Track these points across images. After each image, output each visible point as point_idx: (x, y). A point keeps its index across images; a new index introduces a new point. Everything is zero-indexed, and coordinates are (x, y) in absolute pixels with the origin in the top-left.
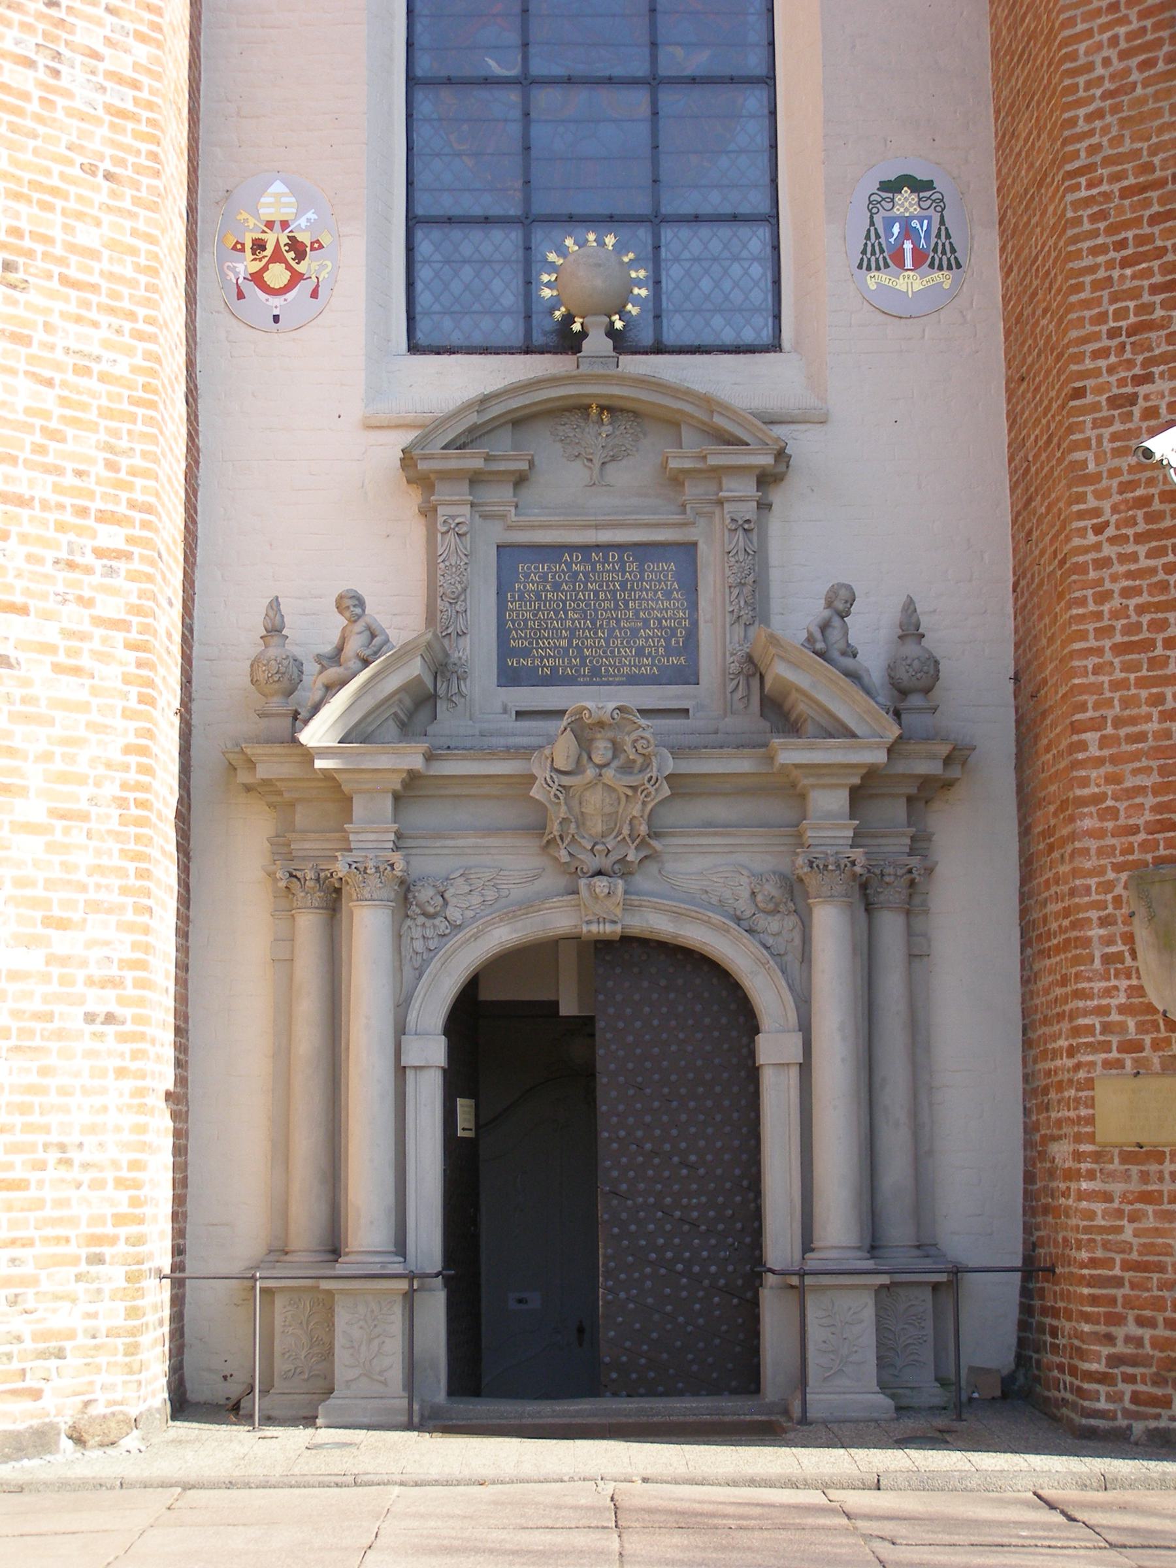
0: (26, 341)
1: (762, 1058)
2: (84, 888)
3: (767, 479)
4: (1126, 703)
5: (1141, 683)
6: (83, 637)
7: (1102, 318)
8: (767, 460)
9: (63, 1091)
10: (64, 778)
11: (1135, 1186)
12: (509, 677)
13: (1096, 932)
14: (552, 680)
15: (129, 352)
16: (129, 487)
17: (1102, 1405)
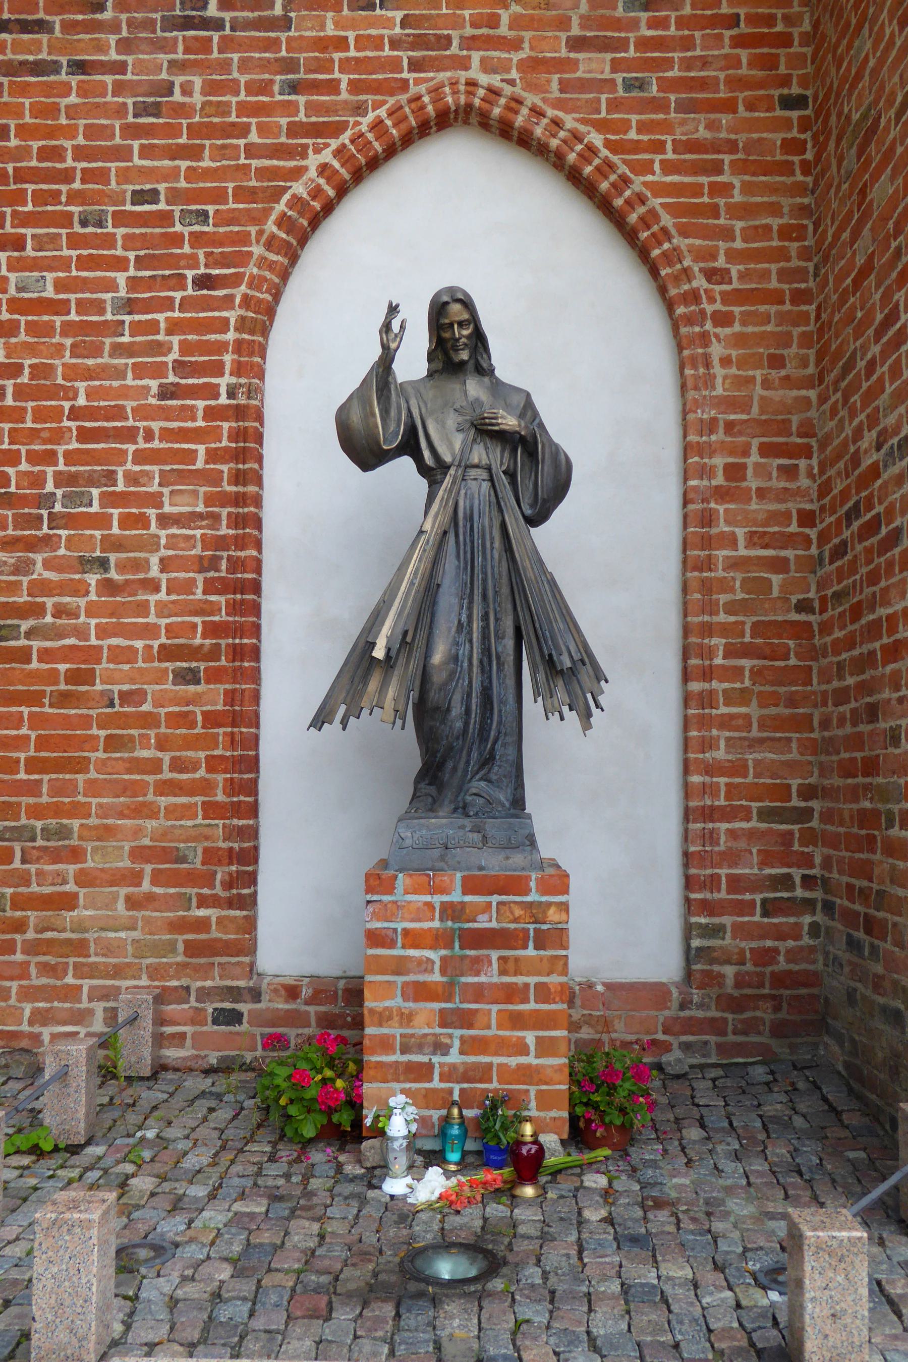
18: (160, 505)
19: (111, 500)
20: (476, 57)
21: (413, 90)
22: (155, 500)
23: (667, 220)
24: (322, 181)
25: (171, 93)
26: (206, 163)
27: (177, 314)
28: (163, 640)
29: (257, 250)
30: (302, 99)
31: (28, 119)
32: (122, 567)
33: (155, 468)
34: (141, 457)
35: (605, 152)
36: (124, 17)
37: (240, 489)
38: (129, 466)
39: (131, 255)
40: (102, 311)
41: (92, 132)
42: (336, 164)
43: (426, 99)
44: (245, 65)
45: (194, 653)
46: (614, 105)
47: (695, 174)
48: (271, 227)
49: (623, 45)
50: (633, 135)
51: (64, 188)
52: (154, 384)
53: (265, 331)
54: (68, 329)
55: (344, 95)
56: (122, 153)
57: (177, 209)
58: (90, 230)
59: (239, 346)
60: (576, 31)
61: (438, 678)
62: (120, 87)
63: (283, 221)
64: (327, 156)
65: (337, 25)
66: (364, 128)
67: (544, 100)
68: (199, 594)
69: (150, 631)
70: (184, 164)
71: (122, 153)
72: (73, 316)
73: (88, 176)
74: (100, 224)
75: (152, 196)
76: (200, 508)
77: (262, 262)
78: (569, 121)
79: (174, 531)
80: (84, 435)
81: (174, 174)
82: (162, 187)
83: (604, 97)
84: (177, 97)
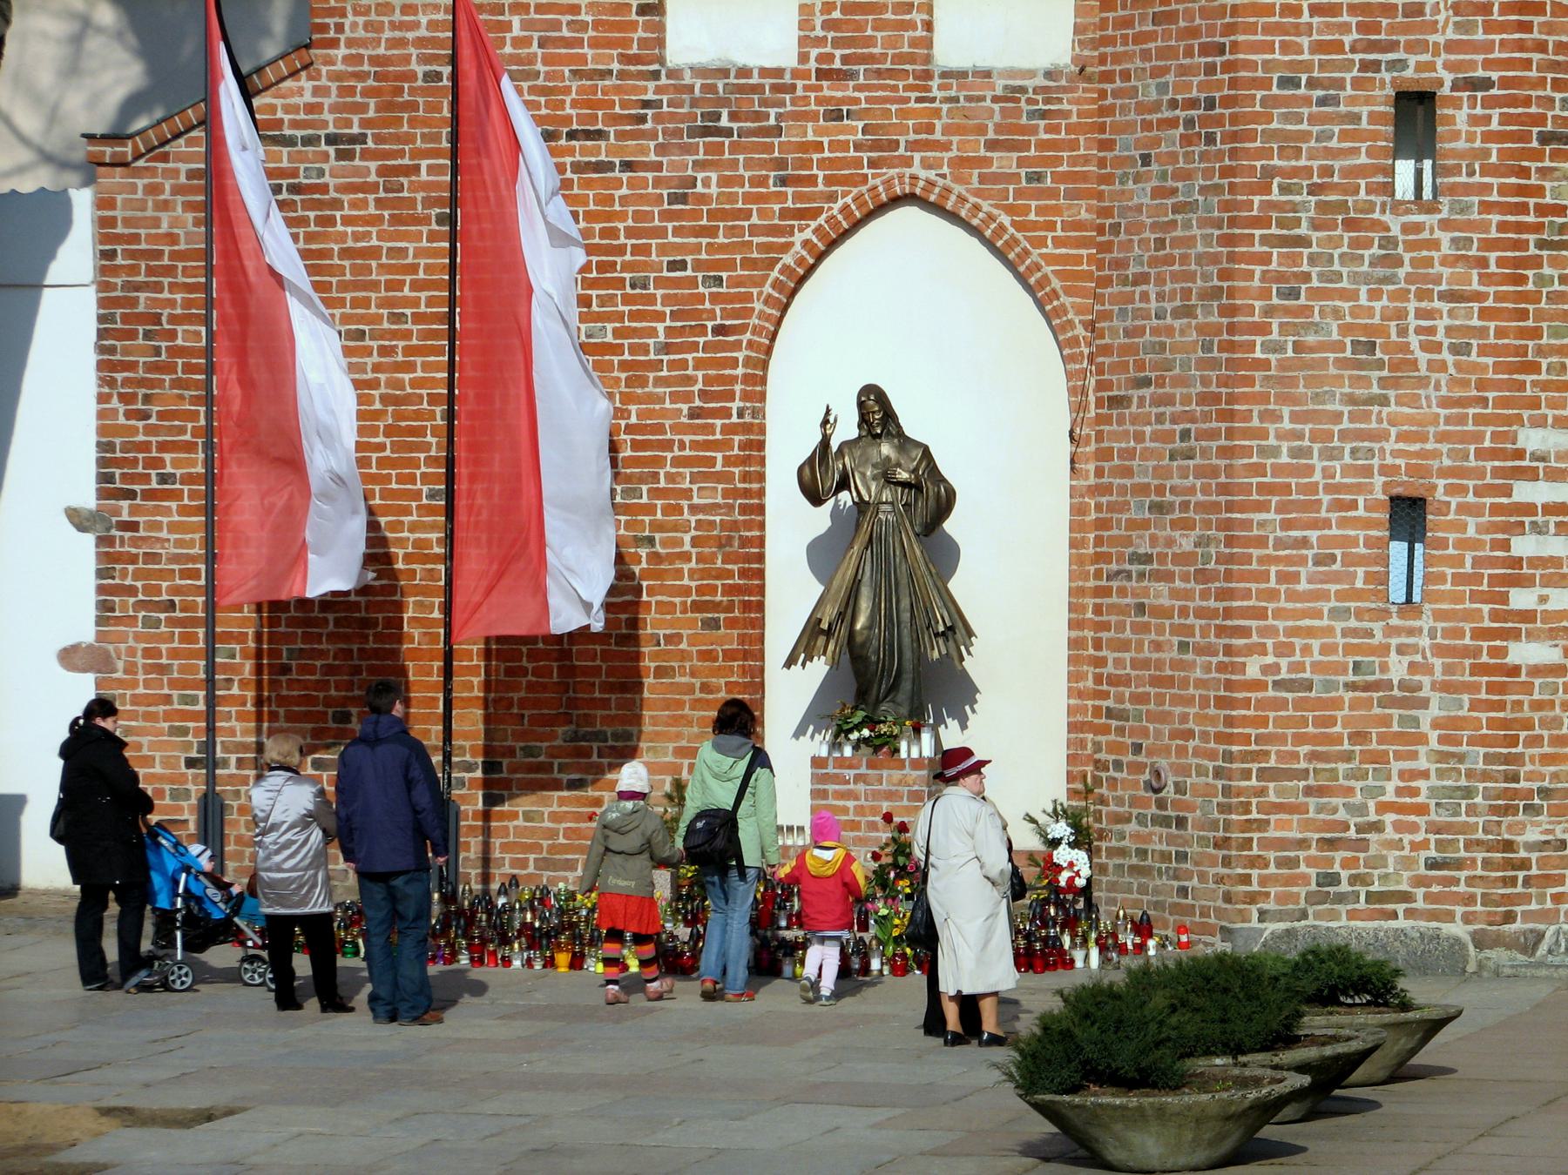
18: (691, 498)
19: (656, 493)
20: (917, 156)
21: (871, 182)
22: (687, 494)
23: (1056, 283)
24: (804, 253)
25: (695, 186)
26: (721, 240)
27: (701, 354)
28: (694, 597)
29: (758, 306)
30: (790, 190)
31: (592, 207)
32: (664, 543)
33: (687, 471)
34: (677, 462)
35: (1011, 230)
36: (660, 127)
37: (747, 486)
38: (668, 468)
39: (668, 310)
40: (647, 353)
41: (638, 216)
42: (815, 240)
43: (881, 189)
44: (748, 165)
45: (716, 607)
46: (1019, 194)
47: (1078, 247)
48: (767, 289)
49: (1025, 146)
50: (1032, 217)
51: (619, 260)
52: (685, 407)
53: (765, 365)
54: (624, 366)
55: (821, 187)
56: (661, 233)
57: (700, 275)
58: (638, 291)
59: (747, 379)
60: (991, 135)
61: (859, 639)
62: (658, 182)
63: (776, 285)
64: (808, 234)
65: (815, 133)
66: (835, 212)
67: (968, 191)
68: (719, 564)
69: (686, 591)
70: (705, 241)
71: (661, 233)
72: (627, 356)
73: (637, 250)
74: (645, 287)
75: (682, 265)
76: (719, 500)
77: (762, 315)
78: (986, 206)
79: (701, 517)
81: (697, 249)
82: (689, 259)
83: (1011, 188)
84: (700, 189)
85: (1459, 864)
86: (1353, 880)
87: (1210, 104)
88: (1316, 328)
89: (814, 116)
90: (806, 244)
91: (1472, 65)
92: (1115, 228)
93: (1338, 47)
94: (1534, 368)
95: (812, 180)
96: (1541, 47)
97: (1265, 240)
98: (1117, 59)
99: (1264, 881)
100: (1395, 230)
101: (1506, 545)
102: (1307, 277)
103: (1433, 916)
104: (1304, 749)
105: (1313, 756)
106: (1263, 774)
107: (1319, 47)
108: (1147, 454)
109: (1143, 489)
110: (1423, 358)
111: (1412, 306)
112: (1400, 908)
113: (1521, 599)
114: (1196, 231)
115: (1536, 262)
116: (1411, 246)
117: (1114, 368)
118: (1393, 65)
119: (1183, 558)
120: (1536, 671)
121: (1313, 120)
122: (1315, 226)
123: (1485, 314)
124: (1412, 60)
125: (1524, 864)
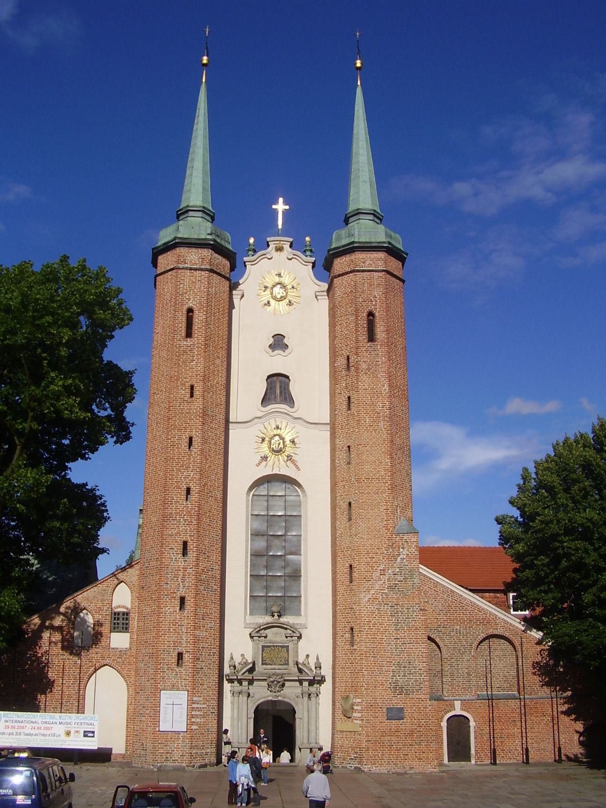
0: (204, 627)
1: (296, 717)
2: (210, 696)
3: (300, 637)
4: (342, 675)
5: (344, 673)
6: (211, 664)
7: (340, 625)
8: (299, 635)
9: (208, 722)
10: (208, 682)
11: (341, 736)
12: (263, 664)
13: (337, 704)
14: (269, 664)
15: (216, 626)
16: (216, 644)
17: (336, 763)
19: (70, 704)
22: (74, 704)
29: (85, 678)
62: (72, 661)
71: (72, 668)
73: (69, 670)
75: (75, 673)
78: (117, 666)
80: (68, 697)
85: (185, 756)
86: (170, 758)
87: (153, 653)
88: (166, 683)
89: (94, 653)
90: (92, 670)
91: (188, 649)
92: (138, 670)
93: (170, 646)
94: (195, 689)
95: (93, 662)
96: (196, 647)
97: (160, 672)
98: (139, 647)
99: (158, 758)
100: (177, 671)
101: (191, 713)
102: (165, 677)
103: (180, 763)
104: (164, 740)
105: (165, 741)
106: (158, 743)
107: (168, 646)
108: (142, 700)
109: (142, 704)
110: (181, 687)
111: (179, 681)
112: (177, 761)
113: (193, 720)
114: (150, 670)
115: (195, 675)
116: (180, 673)
117: (137, 688)
118: (178, 649)
119: (147, 714)
120: (195, 730)
121: (167, 656)
122: (167, 670)
123: (189, 682)
124: (180, 648)
125: (193, 756)
